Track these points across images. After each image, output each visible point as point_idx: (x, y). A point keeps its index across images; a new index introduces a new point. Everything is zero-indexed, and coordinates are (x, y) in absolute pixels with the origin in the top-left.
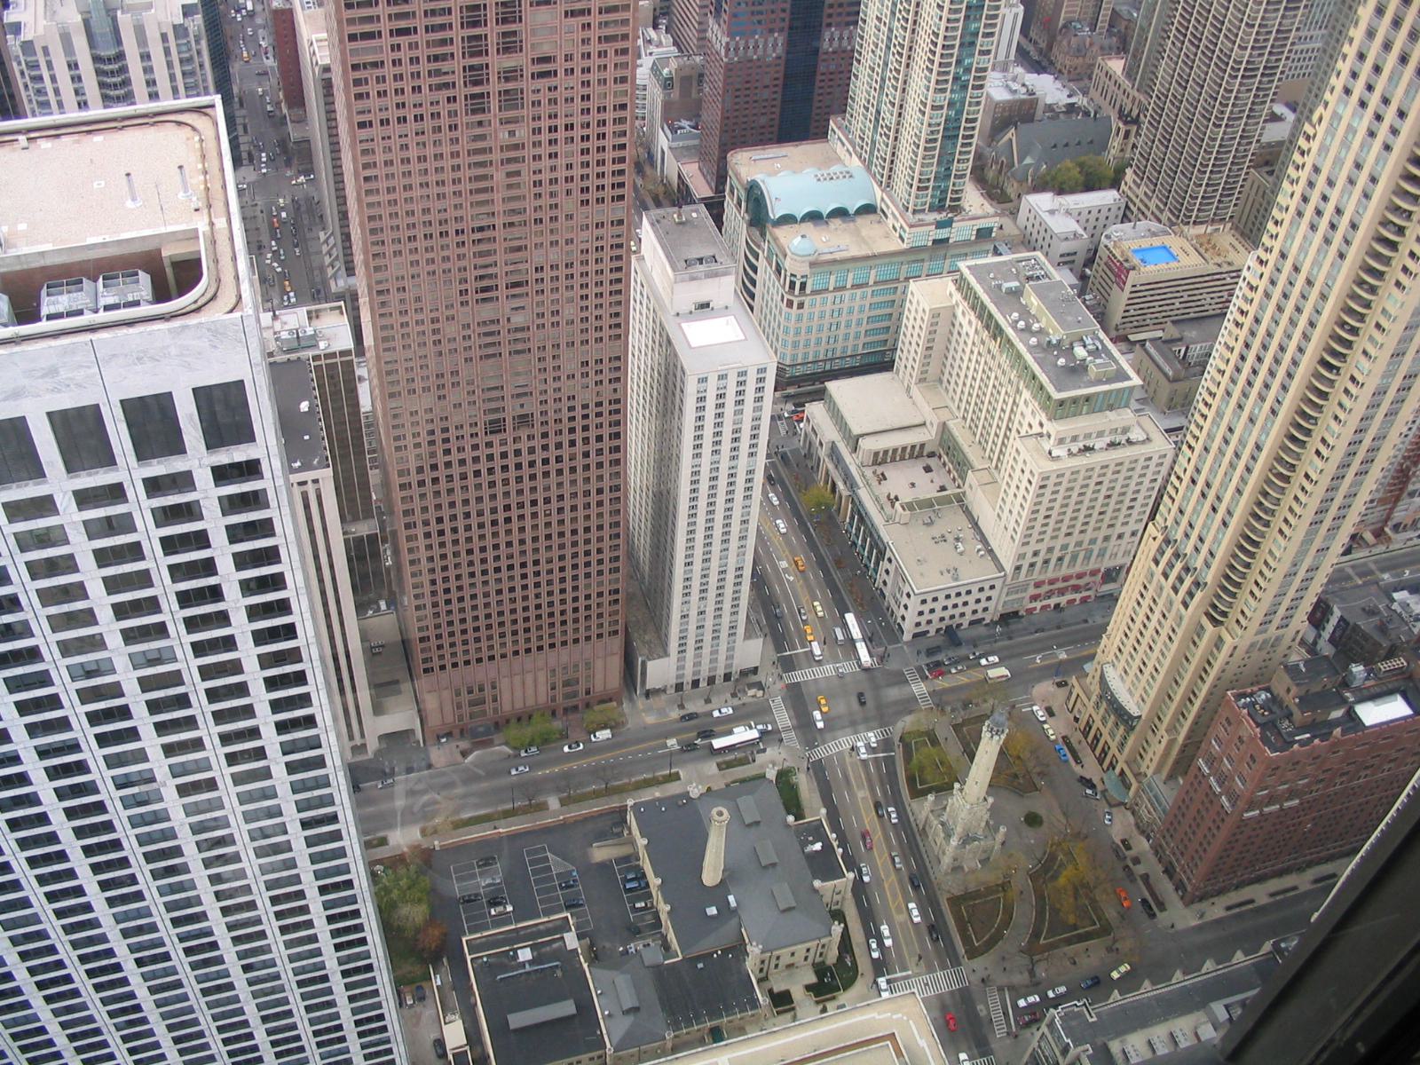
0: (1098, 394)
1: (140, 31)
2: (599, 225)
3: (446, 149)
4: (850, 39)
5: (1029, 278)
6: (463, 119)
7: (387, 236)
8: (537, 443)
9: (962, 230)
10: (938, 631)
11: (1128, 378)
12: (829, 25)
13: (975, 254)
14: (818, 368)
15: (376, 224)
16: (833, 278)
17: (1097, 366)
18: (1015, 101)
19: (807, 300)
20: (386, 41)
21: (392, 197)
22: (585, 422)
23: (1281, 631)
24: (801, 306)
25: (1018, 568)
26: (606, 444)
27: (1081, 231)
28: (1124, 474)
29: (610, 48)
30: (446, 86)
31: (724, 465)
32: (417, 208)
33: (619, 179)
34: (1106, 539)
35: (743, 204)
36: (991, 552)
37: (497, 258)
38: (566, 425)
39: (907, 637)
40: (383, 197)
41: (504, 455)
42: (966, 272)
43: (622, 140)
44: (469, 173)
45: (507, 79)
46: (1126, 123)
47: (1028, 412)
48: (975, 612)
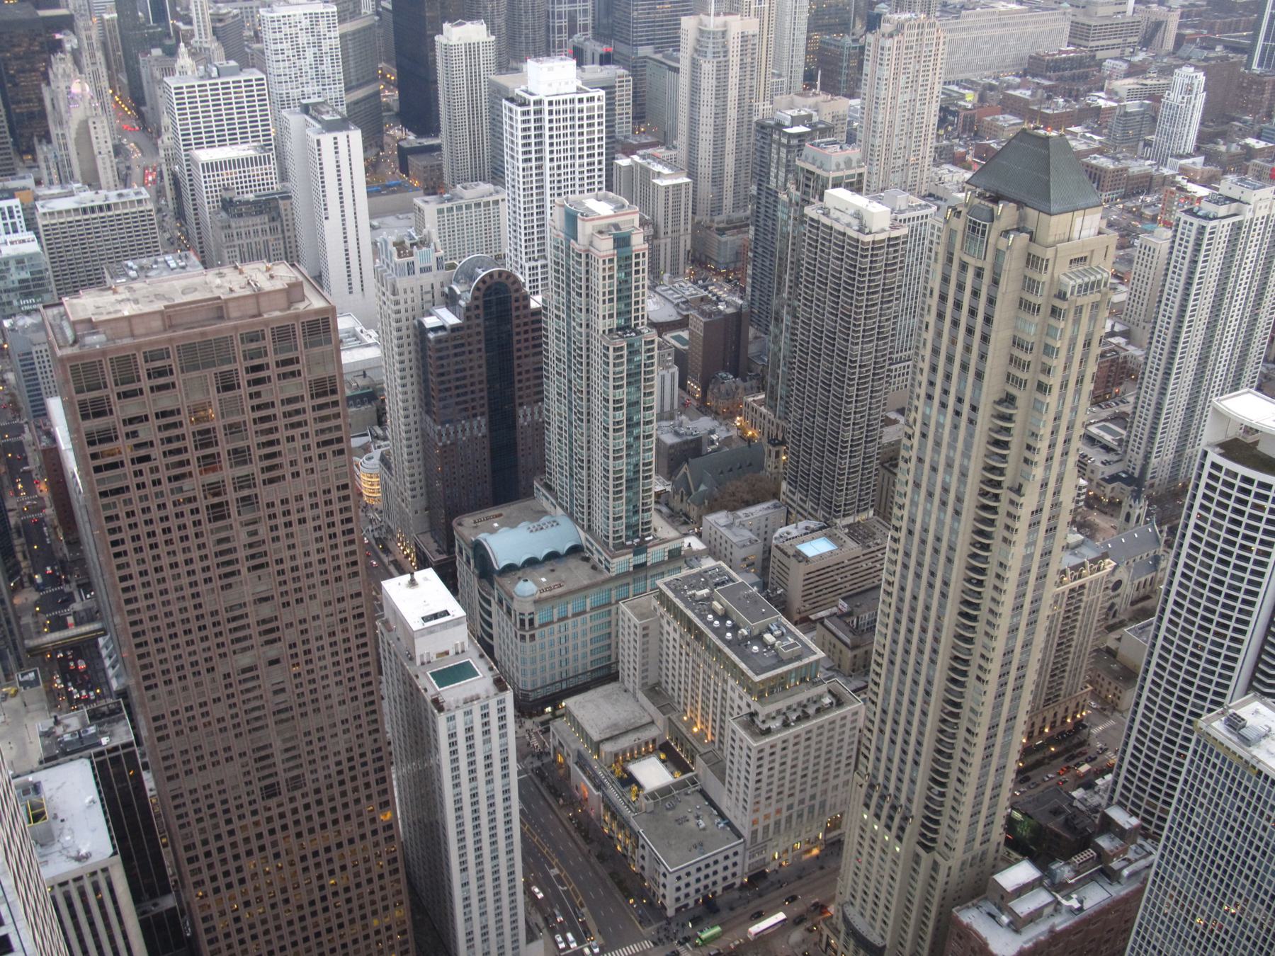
0: (789, 672)
2: (341, 600)
3: (195, 554)
4: (540, 413)
5: (717, 584)
6: (207, 527)
7: (150, 637)
8: (311, 799)
9: (655, 554)
10: (697, 901)
12: (521, 405)
13: (670, 572)
14: (556, 689)
15: (138, 628)
17: (786, 648)
18: (686, 442)
19: (537, 633)
20: (129, 469)
21: (150, 602)
23: (985, 846)
24: (533, 637)
25: (754, 833)
26: (374, 789)
27: (754, 537)
29: (328, 450)
30: (189, 500)
32: (174, 608)
33: (352, 559)
34: (825, 792)
35: (472, 561)
36: (729, 824)
39: (670, 912)
41: (282, 816)
42: (664, 588)
46: (774, 445)
47: (736, 696)
48: (725, 879)
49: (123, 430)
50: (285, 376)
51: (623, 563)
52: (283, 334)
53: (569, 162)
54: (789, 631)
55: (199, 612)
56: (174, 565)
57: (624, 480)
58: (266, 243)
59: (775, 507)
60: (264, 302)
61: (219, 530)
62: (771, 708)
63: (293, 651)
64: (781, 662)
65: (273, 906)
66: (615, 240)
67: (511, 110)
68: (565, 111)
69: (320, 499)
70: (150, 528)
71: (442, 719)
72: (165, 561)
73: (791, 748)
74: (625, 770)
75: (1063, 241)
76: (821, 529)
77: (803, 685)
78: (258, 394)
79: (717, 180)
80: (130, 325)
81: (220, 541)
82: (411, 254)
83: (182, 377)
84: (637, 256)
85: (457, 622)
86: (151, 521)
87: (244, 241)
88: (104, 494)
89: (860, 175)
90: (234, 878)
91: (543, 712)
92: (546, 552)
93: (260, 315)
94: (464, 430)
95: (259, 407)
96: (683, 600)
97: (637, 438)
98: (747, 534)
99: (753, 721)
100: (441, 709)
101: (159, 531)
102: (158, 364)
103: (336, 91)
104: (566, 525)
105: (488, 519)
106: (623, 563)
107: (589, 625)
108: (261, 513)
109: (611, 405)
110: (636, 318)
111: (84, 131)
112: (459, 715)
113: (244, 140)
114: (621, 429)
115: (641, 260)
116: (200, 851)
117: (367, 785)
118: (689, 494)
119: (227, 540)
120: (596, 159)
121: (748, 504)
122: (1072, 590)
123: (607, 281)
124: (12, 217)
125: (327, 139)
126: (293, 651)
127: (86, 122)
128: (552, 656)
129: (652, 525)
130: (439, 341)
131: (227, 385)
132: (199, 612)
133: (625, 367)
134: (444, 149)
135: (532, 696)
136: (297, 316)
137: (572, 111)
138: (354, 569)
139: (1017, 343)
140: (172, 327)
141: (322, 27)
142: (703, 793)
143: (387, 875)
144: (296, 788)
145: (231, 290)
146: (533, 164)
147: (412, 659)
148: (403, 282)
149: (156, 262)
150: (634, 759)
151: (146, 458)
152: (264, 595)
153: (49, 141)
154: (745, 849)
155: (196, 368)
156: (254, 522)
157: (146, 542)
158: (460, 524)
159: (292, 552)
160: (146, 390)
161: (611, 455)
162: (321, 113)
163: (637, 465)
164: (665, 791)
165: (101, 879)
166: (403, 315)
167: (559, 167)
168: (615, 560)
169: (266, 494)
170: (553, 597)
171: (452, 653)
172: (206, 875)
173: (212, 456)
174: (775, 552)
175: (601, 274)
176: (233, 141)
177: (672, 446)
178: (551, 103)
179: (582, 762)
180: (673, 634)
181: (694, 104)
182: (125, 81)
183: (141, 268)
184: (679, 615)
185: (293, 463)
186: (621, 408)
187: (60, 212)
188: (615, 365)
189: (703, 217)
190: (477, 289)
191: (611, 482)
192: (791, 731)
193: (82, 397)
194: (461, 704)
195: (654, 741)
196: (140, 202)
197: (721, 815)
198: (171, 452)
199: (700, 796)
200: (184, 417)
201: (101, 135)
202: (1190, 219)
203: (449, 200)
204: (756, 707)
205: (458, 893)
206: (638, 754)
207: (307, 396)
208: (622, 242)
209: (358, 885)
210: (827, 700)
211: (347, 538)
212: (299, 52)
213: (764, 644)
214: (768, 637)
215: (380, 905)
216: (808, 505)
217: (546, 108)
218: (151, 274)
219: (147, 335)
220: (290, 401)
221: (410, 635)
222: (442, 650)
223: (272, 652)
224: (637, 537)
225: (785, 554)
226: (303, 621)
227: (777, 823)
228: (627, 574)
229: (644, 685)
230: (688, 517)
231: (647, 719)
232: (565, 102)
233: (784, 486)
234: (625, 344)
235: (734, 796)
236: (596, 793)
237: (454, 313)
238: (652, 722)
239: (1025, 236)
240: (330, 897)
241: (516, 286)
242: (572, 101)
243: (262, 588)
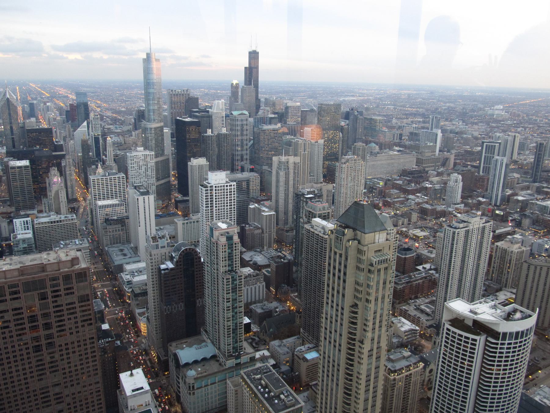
2: (90, 385)
3: (27, 366)
4: (202, 302)
5: (265, 373)
6: (32, 355)
9: (244, 359)
11: (300, 404)
12: (198, 298)
13: (251, 366)
16: (217, 378)
17: (288, 401)
18: (265, 312)
19: (196, 392)
24: (194, 393)
29: (86, 323)
30: (26, 344)
33: (95, 368)
37: (51, 403)
42: (243, 374)
43: (94, 354)
44: (37, 373)
45: (48, 339)
46: (299, 314)
50: (68, 294)
51: (231, 363)
52: (67, 278)
54: (291, 393)
58: (120, 235)
59: (298, 338)
60: (61, 265)
61: (37, 356)
63: (69, 407)
66: (227, 238)
68: (221, 190)
75: (371, 244)
76: (314, 348)
78: (56, 301)
79: (286, 213)
80: (5, 274)
81: (38, 361)
82: (158, 241)
83: (24, 294)
84: (236, 244)
85: (146, 392)
87: (111, 234)
89: (329, 213)
92: (202, 357)
93: (59, 270)
94: (175, 308)
95: (57, 306)
96: (250, 380)
97: (236, 313)
98: (286, 349)
101: (11, 357)
102: (14, 289)
104: (210, 345)
105: (182, 343)
106: (231, 363)
107: (217, 388)
108: (56, 349)
109: (225, 300)
110: (236, 267)
111: (57, 193)
113: (116, 197)
114: (230, 310)
118: (266, 332)
119: (41, 360)
120: (233, 206)
121: (289, 337)
122: (407, 376)
123: (224, 253)
124: (27, 224)
125: (141, 198)
126: (69, 407)
127: (58, 191)
128: (202, 401)
130: (165, 274)
131: (43, 297)
133: (231, 286)
134: (190, 201)
136: (73, 271)
137: (224, 190)
138: (96, 372)
139: (357, 283)
140: (22, 275)
141: (148, 159)
145: (49, 260)
146: (209, 208)
147: (127, 408)
148: (154, 252)
149: (72, 242)
151: (7, 327)
152: (56, 383)
155: (30, 291)
156: (53, 353)
158: (171, 346)
161: (226, 320)
162: (140, 189)
163: (236, 324)
166: (154, 264)
167: (219, 209)
168: (228, 362)
169: (58, 341)
170: (202, 377)
171: (144, 405)
173: (35, 326)
174: (296, 357)
175: (221, 251)
176: (112, 198)
177: (260, 314)
181: (277, 186)
182: (83, 176)
183: (66, 244)
184: (249, 386)
185: (70, 329)
186: (229, 301)
187: (42, 223)
188: (227, 285)
189: (281, 226)
190: (180, 254)
191: (226, 330)
196: (72, 219)
198: (18, 325)
201: (63, 195)
202: (450, 229)
203: (187, 220)
207: (77, 302)
208: (230, 238)
212: (140, 167)
213: (280, 399)
216: (310, 338)
217: (214, 188)
218: (69, 246)
219: (11, 278)
220: (69, 304)
221: (126, 398)
222: (140, 404)
224: (237, 352)
225: (299, 358)
226: (73, 394)
232: (221, 186)
233: (301, 330)
237: (172, 263)
239: (356, 242)
242: (224, 186)
243: (55, 380)
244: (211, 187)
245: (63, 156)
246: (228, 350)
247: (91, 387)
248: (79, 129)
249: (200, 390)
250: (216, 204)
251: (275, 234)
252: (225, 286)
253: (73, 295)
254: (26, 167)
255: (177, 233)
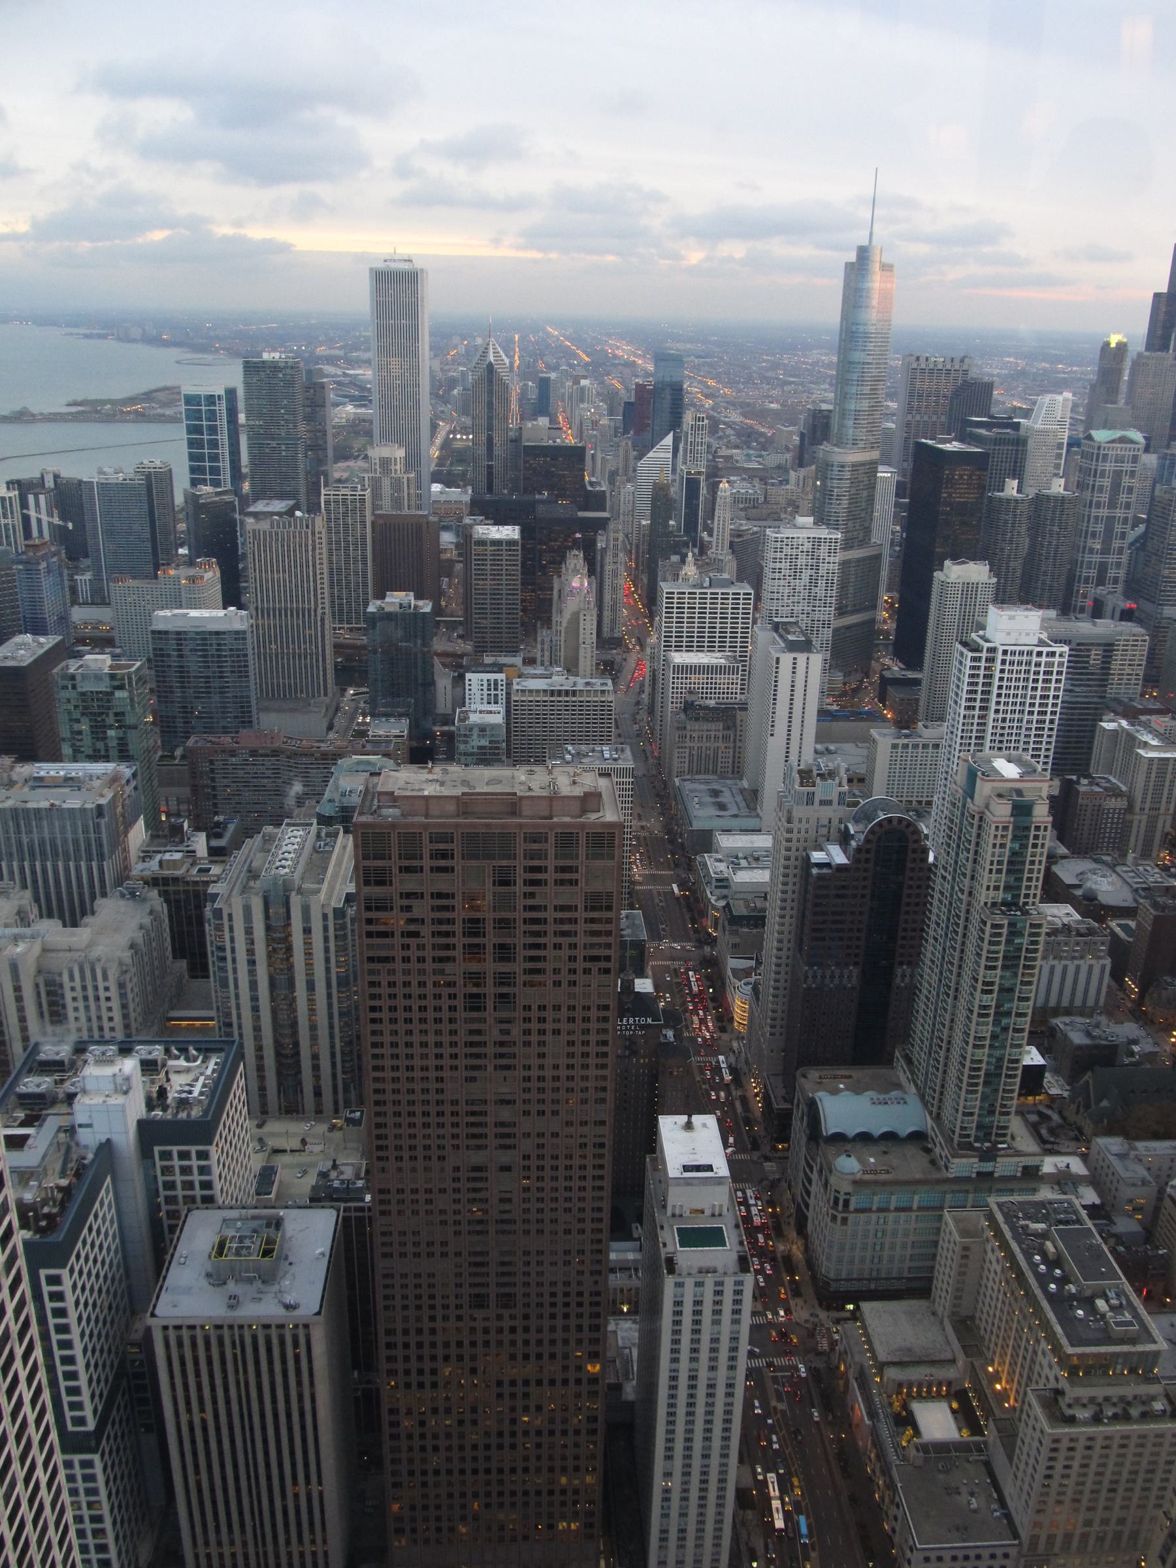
0: (1116, 1355)
1: (306, 911)
3: (446, 1039)
4: (912, 976)
5: (1060, 1222)
6: (461, 1014)
7: (389, 1109)
9: (1004, 1166)
11: (1155, 1342)
12: (901, 964)
13: (1021, 1191)
14: (856, 1286)
16: (916, 1198)
17: (1118, 1324)
18: (1097, 1047)
19: (851, 1217)
20: (398, 940)
22: (553, 1310)
24: (845, 1221)
25: (1034, 1540)
28: (1149, 1449)
29: (595, 966)
30: (449, 984)
31: (703, 1375)
32: (418, 1086)
33: (602, 1084)
36: (1008, 1516)
38: (547, 1310)
40: (388, 1074)
42: (995, 1208)
43: (604, 1049)
44: (465, 1062)
47: (1045, 1363)
49: (399, 902)
50: (562, 882)
51: (964, 1166)
52: (567, 840)
53: (1017, 716)
55: (440, 1097)
56: (424, 1045)
57: (982, 1073)
58: (716, 750)
61: (472, 1021)
62: (1084, 1393)
63: (526, 1163)
64: (1109, 1340)
65: (461, 1423)
67: (962, 654)
68: (1020, 663)
69: (579, 1014)
70: (407, 1003)
71: (669, 1282)
72: (416, 1038)
73: (1115, 1449)
74: (905, 1406)
77: (1133, 1376)
78: (532, 895)
81: (472, 1032)
85: (719, 1181)
86: (410, 996)
87: (696, 745)
88: (371, 959)
90: (427, 1379)
91: (843, 1309)
93: (551, 817)
94: (832, 977)
95: (532, 908)
96: (1013, 1228)
97: (1005, 1029)
98: (1142, 1172)
99: (1056, 1401)
100: (671, 1270)
101: (415, 1008)
102: (442, 846)
103: (827, 613)
105: (835, 1077)
106: (964, 1166)
108: (516, 1014)
109: (979, 986)
110: (1027, 896)
111: (575, 619)
112: (689, 1283)
113: (722, 648)
114: (987, 1015)
115: (1041, 833)
116: (399, 1338)
117: (579, 1328)
118: (1087, 1106)
119: (479, 1032)
120: (1048, 717)
121: (1157, 1136)
123: (997, 850)
125: (787, 659)
126: (526, 1163)
128: (864, 1248)
129: (1009, 1132)
130: (820, 877)
131: (504, 880)
132: (440, 1097)
133: (1002, 947)
135: (834, 1286)
136: (583, 826)
137: (1029, 663)
140: (466, 814)
141: (823, 551)
142: (988, 1466)
143: (584, 1432)
144: (506, 1306)
145: (530, 789)
146: (977, 712)
147: (664, 1207)
148: (800, 812)
150: (920, 1397)
151: (416, 934)
152: (507, 1098)
153: (550, 628)
154: (1020, 1555)
155: (474, 856)
156: (508, 1021)
157: (401, 1015)
158: (804, 1076)
159: (541, 1061)
160: (427, 868)
162: (788, 633)
163: (1000, 1059)
164: (942, 1448)
165: (301, 1332)
166: (794, 845)
167: (1004, 720)
168: (956, 1160)
169: (525, 995)
170: (876, 1183)
171: (708, 1212)
172: (400, 1366)
173: (478, 945)
174: (1168, 1203)
175: (991, 841)
176: (711, 649)
178: (1005, 652)
179: (863, 1380)
180: (995, 1265)
182: (645, 580)
183: (578, 753)
184: (1004, 1246)
185: (556, 971)
186: (990, 992)
187: (531, 691)
188: (990, 943)
190: (872, 831)
191: (966, 1071)
192: (1101, 1428)
193: (367, 863)
194: (694, 1271)
195: (949, 1384)
196: (603, 692)
197: (1002, 1502)
198: (440, 934)
199: (983, 1469)
200: (457, 902)
201: (588, 626)
203: (906, 736)
204: (1064, 1384)
205: (659, 1483)
206: (928, 1393)
207: (581, 907)
208: (1022, 810)
209: (552, 1433)
210: (1158, 1406)
211: (600, 1061)
212: (796, 573)
214: (1101, 1304)
215: (570, 1463)
217: (1000, 657)
218: (585, 760)
220: (563, 908)
221: (664, 1180)
223: (505, 1158)
226: (541, 1135)
227: (1085, 1537)
228: (968, 1179)
229: (953, 1313)
230: (1082, 1133)
231: (949, 1356)
232: (1021, 653)
234: (1006, 922)
235: (1019, 1483)
236: (867, 1422)
237: (845, 852)
238: (953, 1361)
240: (519, 1434)
241: (915, 837)
242: (1030, 653)
244: (992, 650)
245: (602, 524)
246: (962, 1128)
247: (585, 1130)
248: (651, 454)
249: (863, 1217)
250: (998, 703)
251: (1169, 819)
252: (985, 946)
253: (574, 889)
254: (511, 543)
255: (871, 771)
